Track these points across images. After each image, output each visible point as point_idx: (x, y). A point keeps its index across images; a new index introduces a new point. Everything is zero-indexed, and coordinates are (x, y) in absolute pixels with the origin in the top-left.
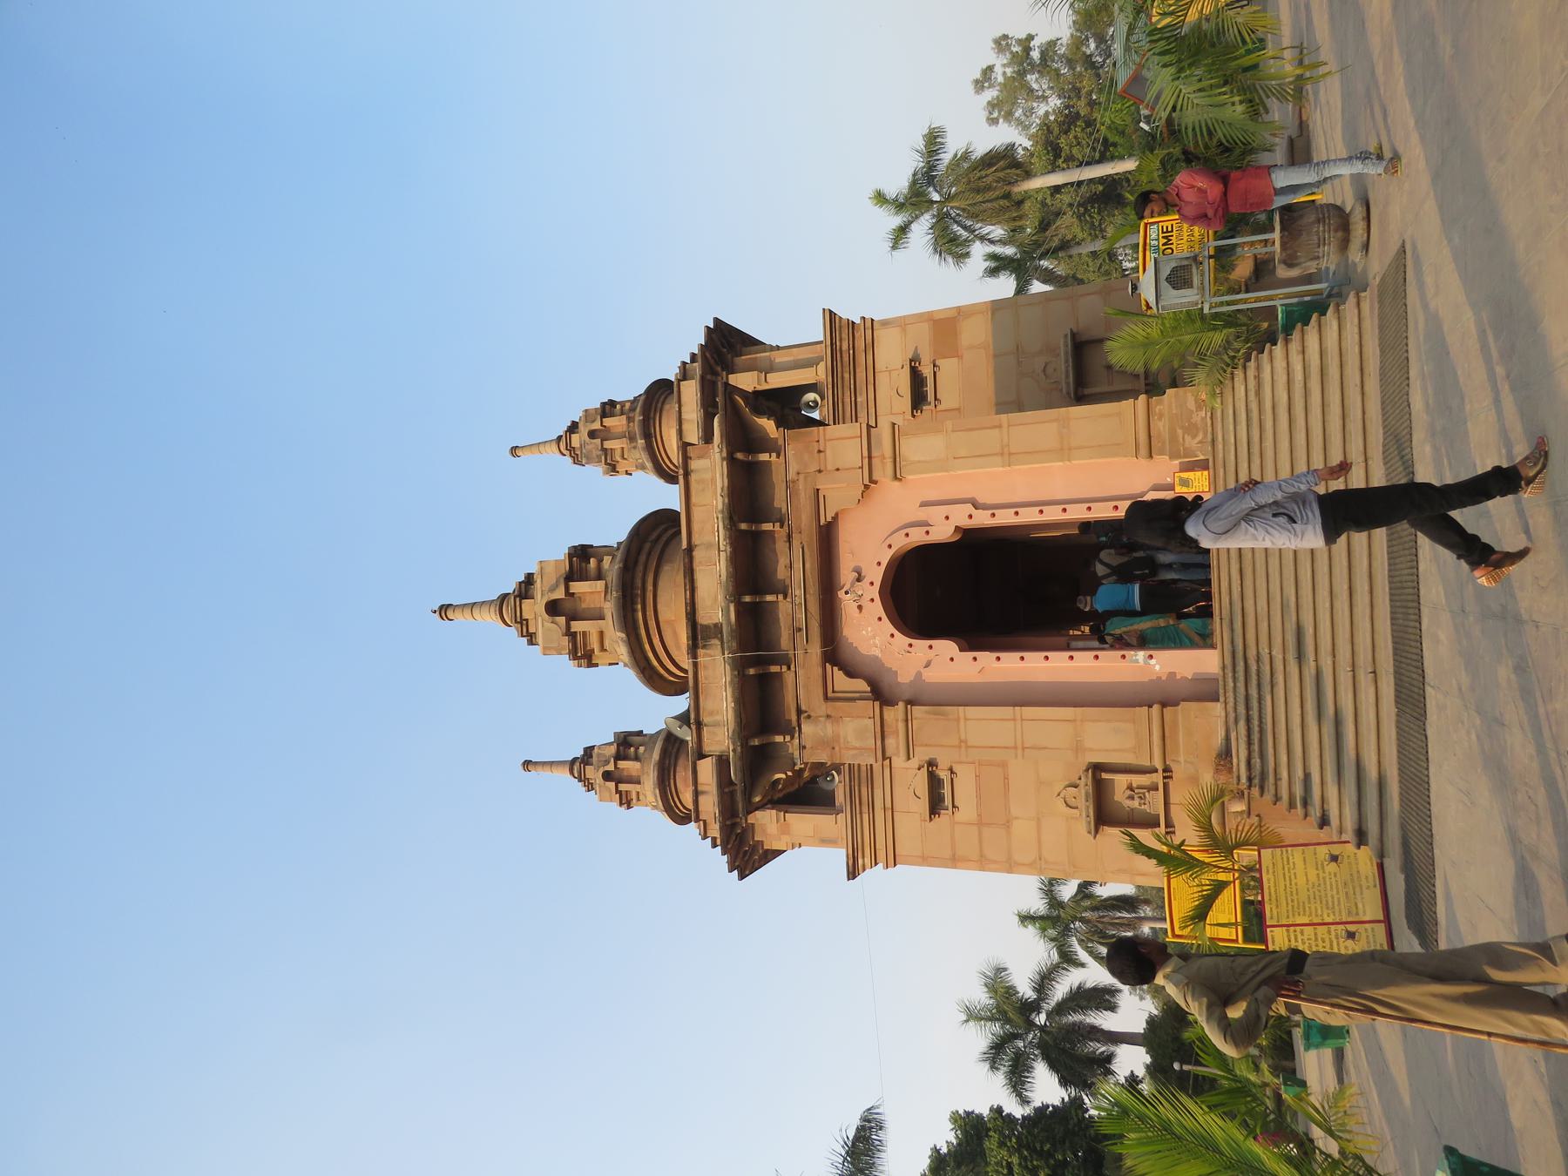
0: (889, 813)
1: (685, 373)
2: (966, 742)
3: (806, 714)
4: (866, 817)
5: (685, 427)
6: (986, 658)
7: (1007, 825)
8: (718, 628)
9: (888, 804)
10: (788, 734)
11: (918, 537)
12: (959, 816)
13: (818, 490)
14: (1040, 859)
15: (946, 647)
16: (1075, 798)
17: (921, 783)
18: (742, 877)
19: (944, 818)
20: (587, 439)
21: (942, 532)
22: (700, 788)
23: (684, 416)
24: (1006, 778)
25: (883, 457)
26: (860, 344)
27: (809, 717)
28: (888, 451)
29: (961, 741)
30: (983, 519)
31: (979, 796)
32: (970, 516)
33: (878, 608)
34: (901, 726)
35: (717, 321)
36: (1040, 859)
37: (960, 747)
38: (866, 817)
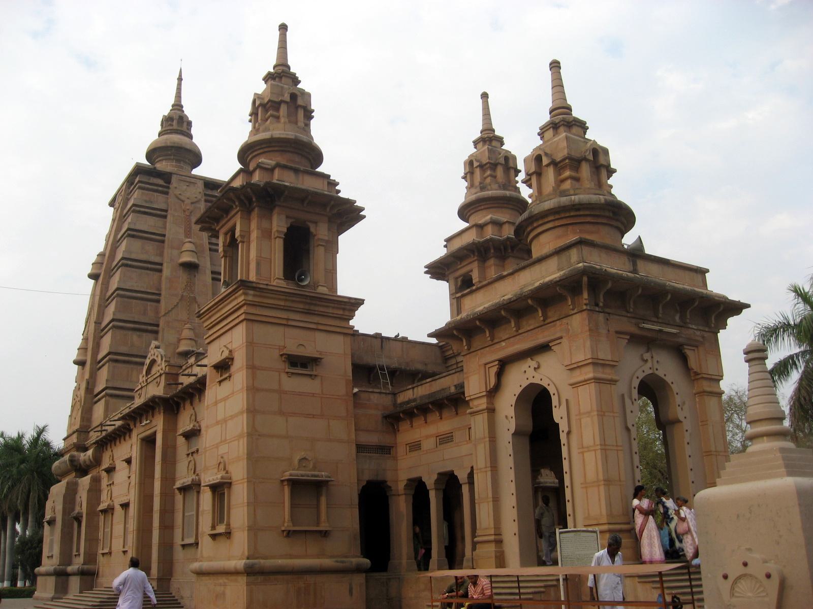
0: (284, 322)
2: (604, 415)
3: (608, 318)
4: (282, 303)
7: (281, 413)
10: (589, 301)
12: (284, 377)
14: (259, 435)
16: (304, 466)
17: (308, 351)
19: (282, 365)
22: (301, 176)
24: (314, 416)
27: (607, 319)
29: (604, 412)
31: (300, 394)
32: (687, 431)
36: (259, 435)
37: (602, 411)
38: (282, 303)
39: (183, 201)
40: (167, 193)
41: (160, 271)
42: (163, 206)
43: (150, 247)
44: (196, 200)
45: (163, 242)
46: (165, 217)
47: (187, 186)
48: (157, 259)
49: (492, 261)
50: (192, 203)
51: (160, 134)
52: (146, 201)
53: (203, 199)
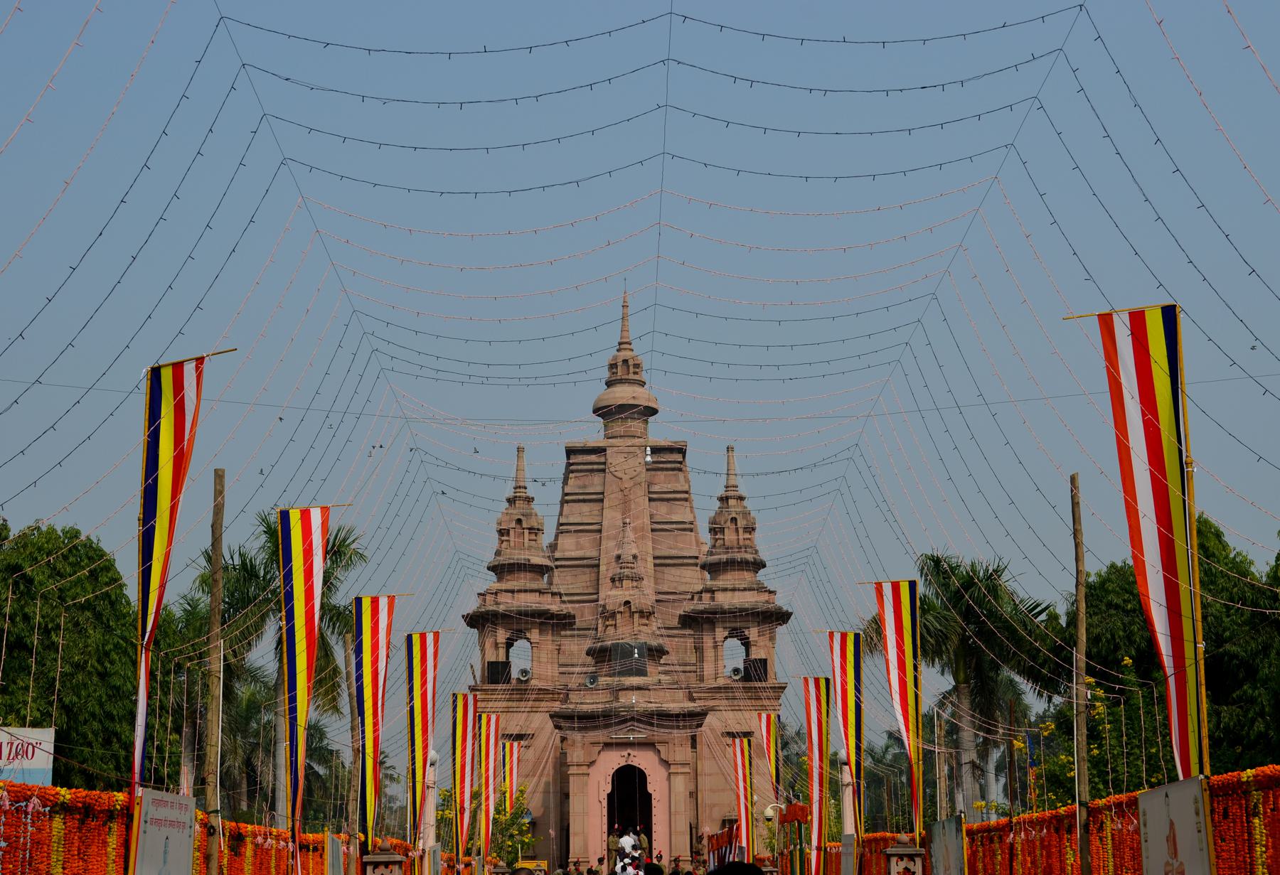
0: (506, 710)
1: (761, 589)
5: (729, 594)
6: (605, 803)
8: (617, 699)
9: (511, 710)
11: (649, 779)
13: (668, 743)
15: (609, 789)
18: (463, 616)
20: (731, 516)
21: (650, 789)
23: (737, 593)
25: (678, 768)
26: (766, 703)
28: (679, 771)
30: (654, 803)
33: (623, 764)
34: (581, 772)
35: (791, 614)
39: (621, 479)
40: (604, 471)
41: (598, 566)
42: (599, 489)
43: (586, 539)
44: (635, 473)
45: (600, 531)
46: (602, 501)
47: (625, 458)
48: (594, 553)
49: (705, 626)
50: (631, 479)
51: (609, 384)
52: (580, 487)
53: (644, 470)
